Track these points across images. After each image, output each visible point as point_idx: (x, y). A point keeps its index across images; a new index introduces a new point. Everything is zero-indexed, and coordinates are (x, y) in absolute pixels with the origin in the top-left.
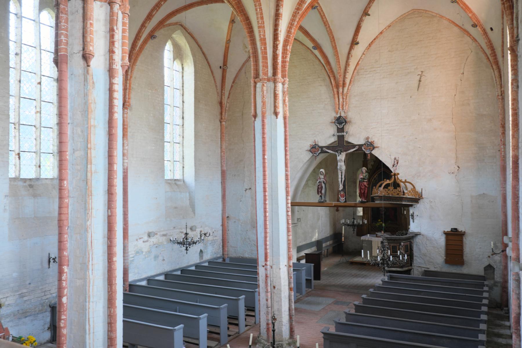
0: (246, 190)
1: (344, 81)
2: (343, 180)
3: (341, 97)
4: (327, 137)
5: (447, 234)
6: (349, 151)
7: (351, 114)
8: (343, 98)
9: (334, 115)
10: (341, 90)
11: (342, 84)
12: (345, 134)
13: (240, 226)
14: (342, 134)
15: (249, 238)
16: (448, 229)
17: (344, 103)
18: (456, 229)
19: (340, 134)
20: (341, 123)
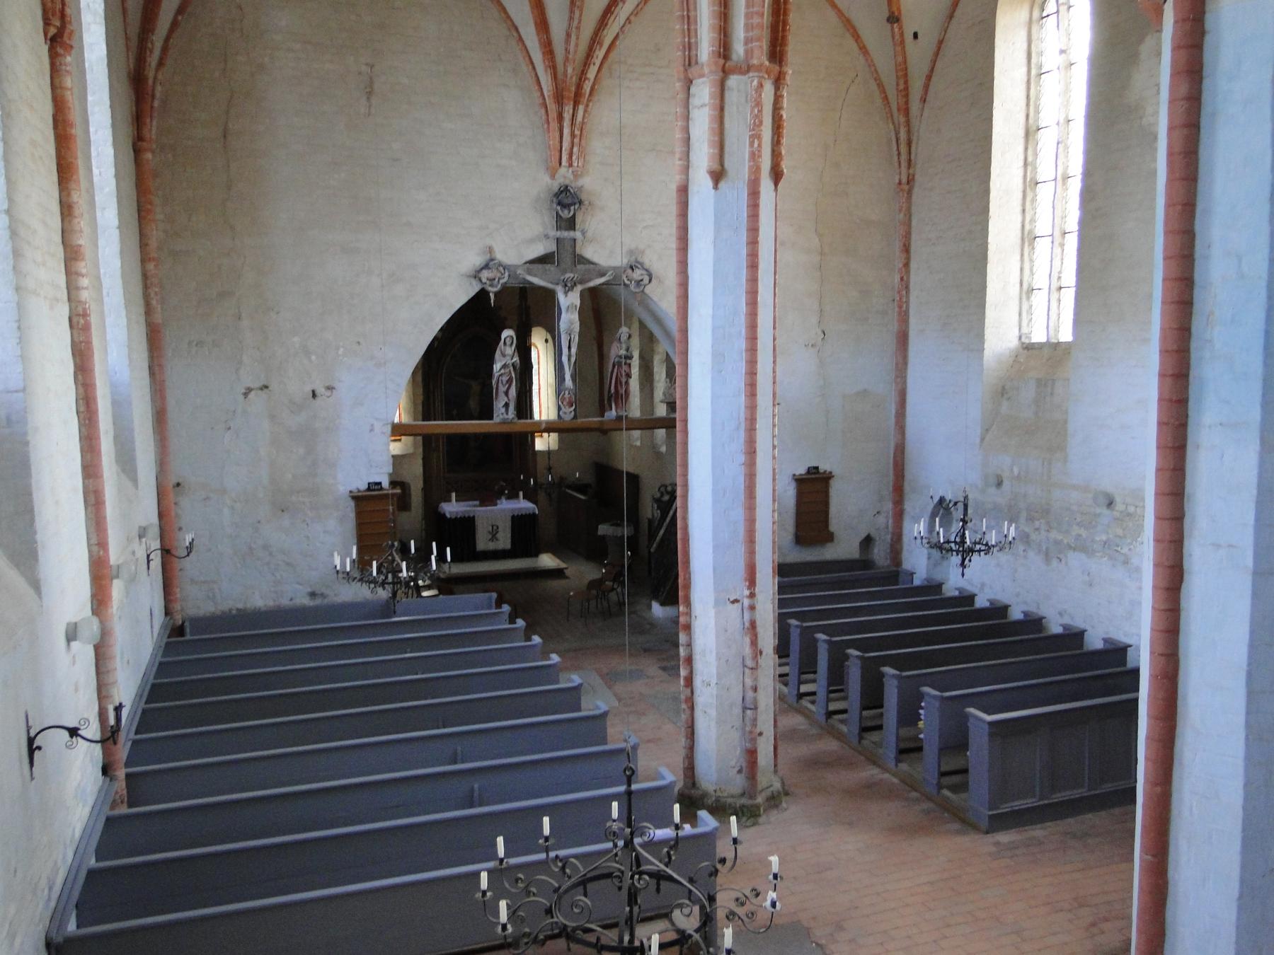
0: (247, 392)
1: (579, 86)
2: (573, 360)
3: (566, 131)
4: (519, 241)
5: (800, 481)
6: (591, 284)
7: (589, 183)
8: (573, 135)
9: (545, 183)
10: (568, 110)
11: (572, 95)
12: (578, 235)
13: (226, 511)
14: (572, 234)
15: (266, 547)
16: (801, 470)
17: (575, 149)
18: (817, 468)
19: (566, 234)
20: (567, 205)
